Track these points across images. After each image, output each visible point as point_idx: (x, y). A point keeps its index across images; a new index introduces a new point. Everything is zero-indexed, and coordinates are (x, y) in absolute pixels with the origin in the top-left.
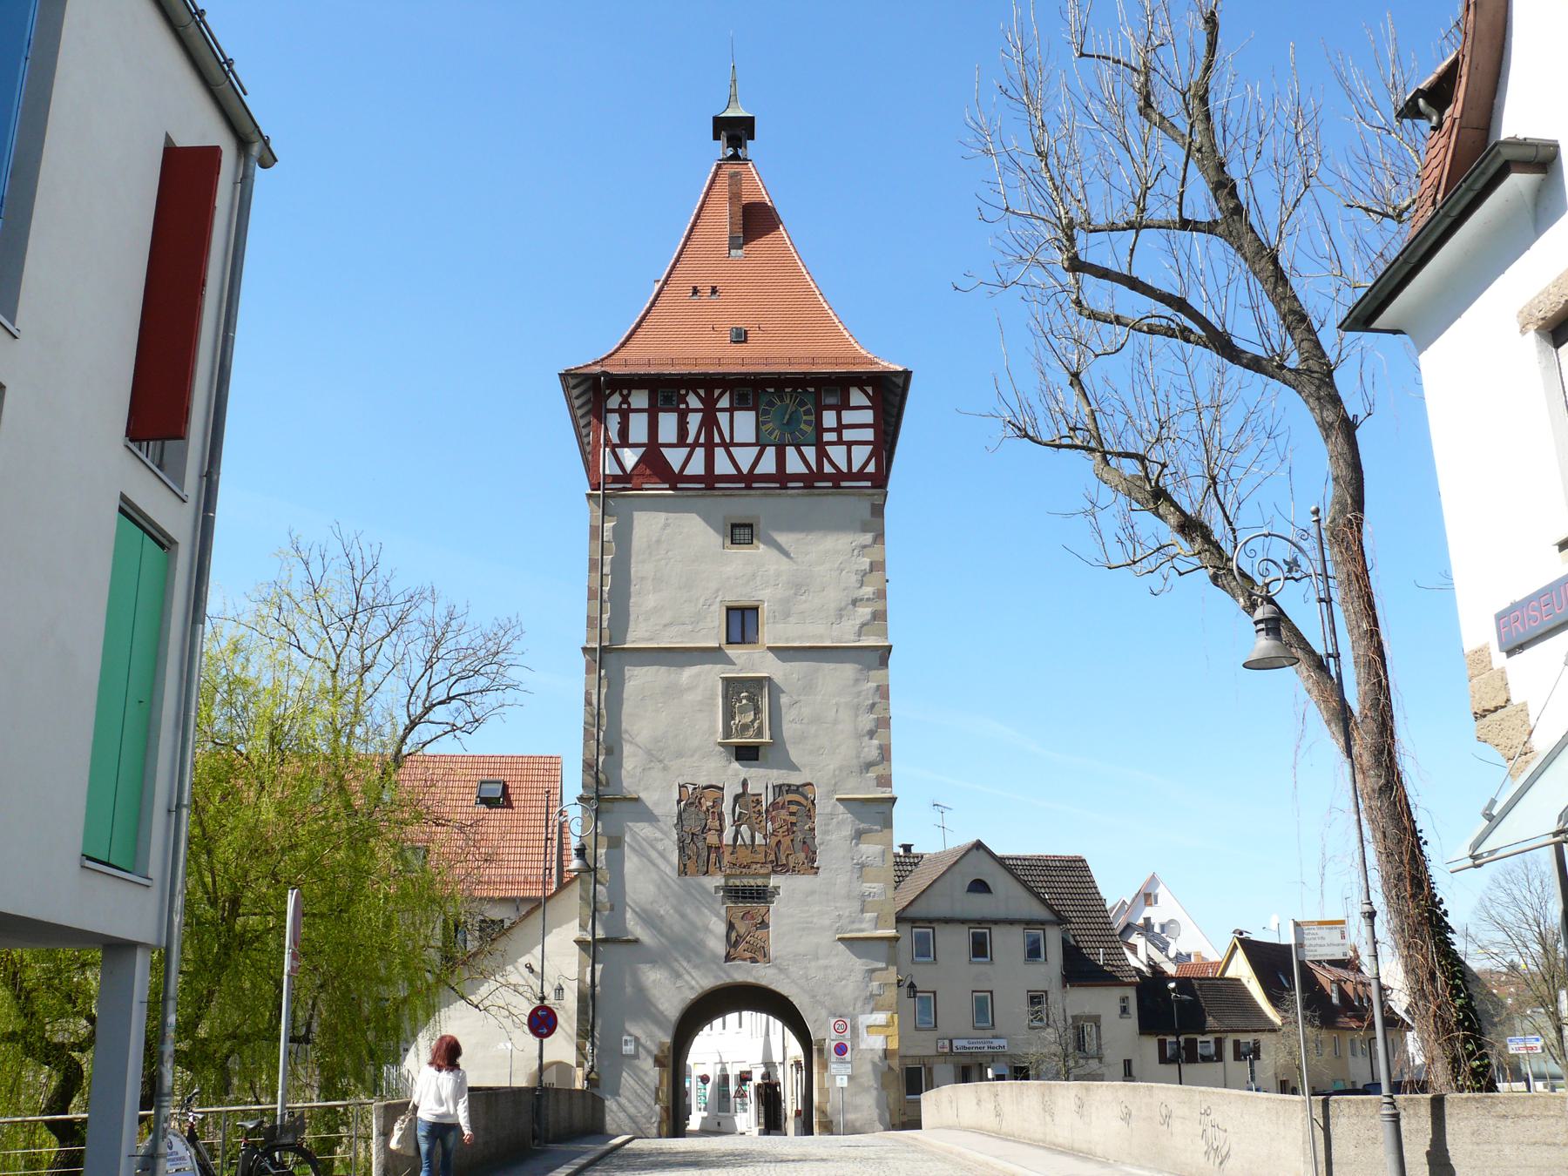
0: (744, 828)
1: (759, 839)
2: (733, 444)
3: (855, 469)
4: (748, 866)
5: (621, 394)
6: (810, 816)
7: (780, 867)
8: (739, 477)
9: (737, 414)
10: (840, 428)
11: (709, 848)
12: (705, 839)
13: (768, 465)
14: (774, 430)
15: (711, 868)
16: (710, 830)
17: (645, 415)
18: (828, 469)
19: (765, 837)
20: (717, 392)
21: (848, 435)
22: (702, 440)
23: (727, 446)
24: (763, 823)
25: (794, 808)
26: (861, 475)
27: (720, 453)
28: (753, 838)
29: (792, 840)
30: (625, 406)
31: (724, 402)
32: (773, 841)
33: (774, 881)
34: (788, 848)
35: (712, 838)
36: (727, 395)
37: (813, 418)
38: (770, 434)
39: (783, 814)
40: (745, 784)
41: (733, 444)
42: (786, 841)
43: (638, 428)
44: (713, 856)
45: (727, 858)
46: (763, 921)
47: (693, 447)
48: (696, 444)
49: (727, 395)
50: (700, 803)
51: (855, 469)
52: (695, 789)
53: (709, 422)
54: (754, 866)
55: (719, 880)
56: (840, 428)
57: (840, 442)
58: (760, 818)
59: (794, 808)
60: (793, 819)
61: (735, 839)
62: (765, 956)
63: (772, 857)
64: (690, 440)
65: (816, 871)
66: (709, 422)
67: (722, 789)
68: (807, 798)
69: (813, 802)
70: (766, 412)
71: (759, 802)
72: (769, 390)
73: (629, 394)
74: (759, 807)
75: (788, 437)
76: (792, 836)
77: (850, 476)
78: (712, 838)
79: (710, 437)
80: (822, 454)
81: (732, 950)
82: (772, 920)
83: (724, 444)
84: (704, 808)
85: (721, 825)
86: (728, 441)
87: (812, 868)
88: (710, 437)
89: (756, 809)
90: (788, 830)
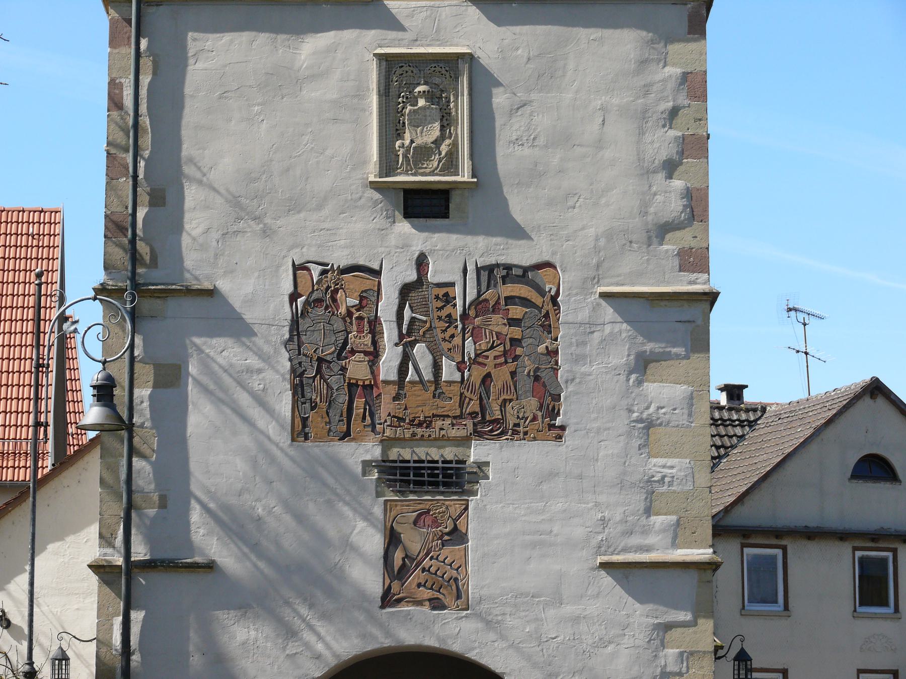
0: (419, 349)
4: (427, 423)
11: (352, 386)
12: (344, 369)
16: (353, 352)
19: (460, 367)
24: (457, 340)
25: (516, 311)
28: (437, 368)
29: (513, 374)
32: (476, 375)
33: (477, 452)
35: (358, 369)
39: (497, 323)
40: (421, 263)
42: (501, 376)
44: (359, 403)
45: (386, 407)
46: (455, 529)
50: (334, 300)
52: (324, 272)
54: (439, 423)
55: (371, 450)
58: (451, 331)
59: (516, 311)
60: (516, 332)
61: (402, 370)
62: (459, 597)
63: (474, 406)
65: (558, 433)
67: (377, 273)
68: (541, 292)
69: (554, 300)
71: (448, 299)
74: (448, 310)
76: (511, 366)
78: (358, 369)
82: (473, 527)
84: (343, 310)
85: (374, 343)
87: (552, 427)
89: (444, 313)
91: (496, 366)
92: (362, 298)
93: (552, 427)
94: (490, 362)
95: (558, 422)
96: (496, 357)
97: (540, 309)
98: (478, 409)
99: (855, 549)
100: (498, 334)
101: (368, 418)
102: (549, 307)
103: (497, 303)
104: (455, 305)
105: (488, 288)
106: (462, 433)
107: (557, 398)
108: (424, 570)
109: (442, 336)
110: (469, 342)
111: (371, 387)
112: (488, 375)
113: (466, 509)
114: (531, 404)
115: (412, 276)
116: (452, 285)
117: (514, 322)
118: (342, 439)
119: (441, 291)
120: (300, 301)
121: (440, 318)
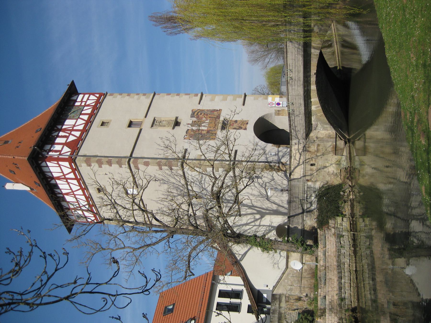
6: (203, 110)
7: (218, 117)
33: (222, 119)
45: (212, 129)
54: (216, 123)
59: (199, 114)
60: (203, 114)
68: (197, 111)
71: (195, 121)
94: (207, 117)
107: (215, 110)
114: (216, 113)
117: (201, 114)
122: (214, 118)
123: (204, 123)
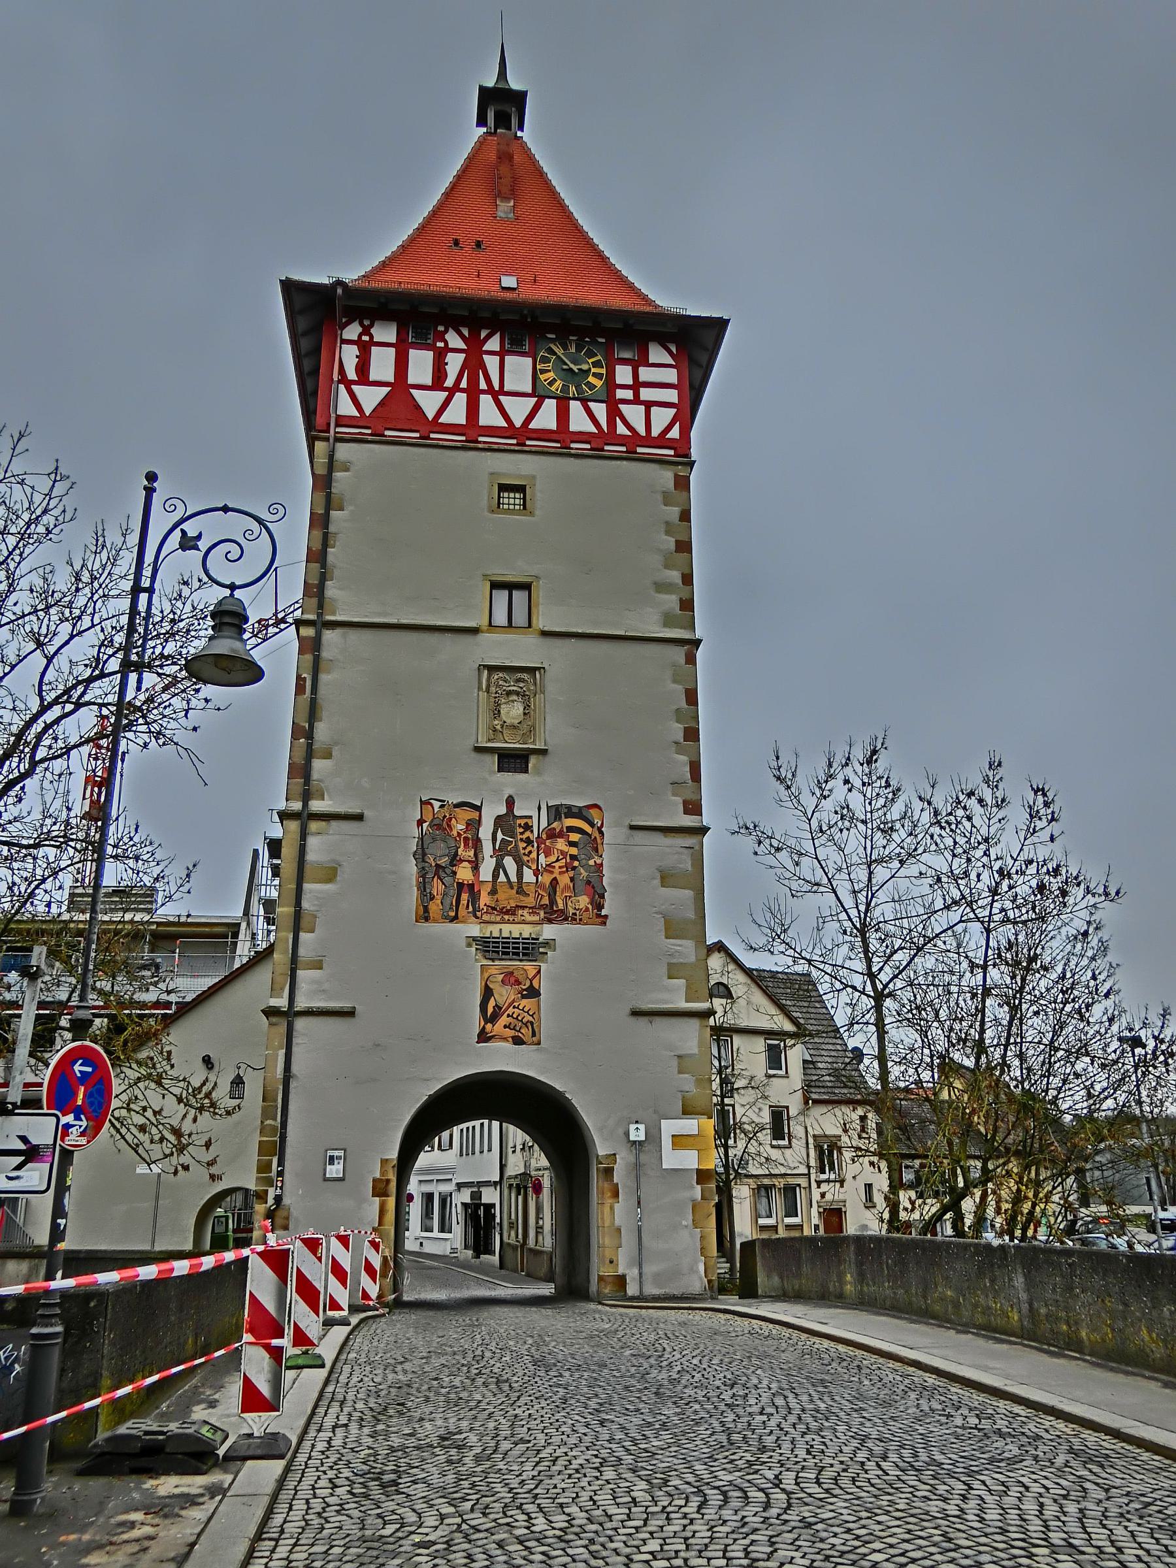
1: (529, 876)
2: (502, 392)
3: (655, 432)
4: (512, 912)
5: (361, 324)
8: (510, 430)
9: (508, 358)
10: (637, 385)
11: (461, 886)
12: (455, 873)
13: (547, 418)
14: (554, 380)
15: (462, 912)
16: (461, 861)
17: (393, 350)
18: (621, 429)
19: (536, 873)
20: (483, 334)
21: (646, 394)
22: (464, 384)
23: (496, 394)
24: (534, 855)
25: (575, 837)
26: (662, 441)
27: (486, 401)
28: (520, 874)
29: (572, 879)
30: (366, 338)
31: (494, 344)
32: (546, 879)
33: (549, 931)
34: (566, 887)
35: (464, 873)
36: (497, 337)
37: (603, 371)
38: (551, 384)
39: (561, 844)
41: (502, 392)
42: (564, 880)
43: (383, 365)
44: (465, 897)
45: (485, 899)
47: (452, 391)
48: (456, 388)
49: (497, 337)
50: (449, 826)
51: (655, 432)
52: (442, 807)
53: (474, 364)
54: (520, 912)
56: (637, 385)
57: (636, 401)
58: (529, 848)
59: (575, 837)
60: (574, 851)
61: (495, 875)
63: (546, 901)
64: (449, 383)
66: (474, 364)
67: (478, 808)
70: (545, 360)
71: (527, 827)
72: (549, 336)
73: (372, 325)
74: (528, 834)
75: (572, 390)
76: (571, 874)
77: (648, 441)
78: (464, 873)
79: (473, 382)
80: (614, 413)
81: (489, 1026)
83: (490, 390)
85: (476, 855)
86: (497, 387)
87: (599, 916)
88: (473, 382)
90: (566, 866)
91: (560, 873)
92: (468, 825)
93: (599, 916)
94: (557, 870)
95: (603, 912)
96: (560, 867)
97: (590, 836)
98: (548, 903)
99: (765, 1039)
100: (562, 852)
101: (470, 907)
102: (596, 834)
103: (561, 831)
104: (532, 831)
105: (555, 820)
106: (536, 918)
107: (602, 896)
108: (508, 1016)
109: (523, 852)
110: (542, 857)
111: (473, 885)
112: (555, 879)
113: (539, 972)
114: (584, 901)
115: (503, 810)
116: (531, 817)
117: (572, 844)
118: (451, 921)
119: (523, 822)
120: (425, 825)
121: (521, 840)
122: (553, 901)
123: (520, 865)
